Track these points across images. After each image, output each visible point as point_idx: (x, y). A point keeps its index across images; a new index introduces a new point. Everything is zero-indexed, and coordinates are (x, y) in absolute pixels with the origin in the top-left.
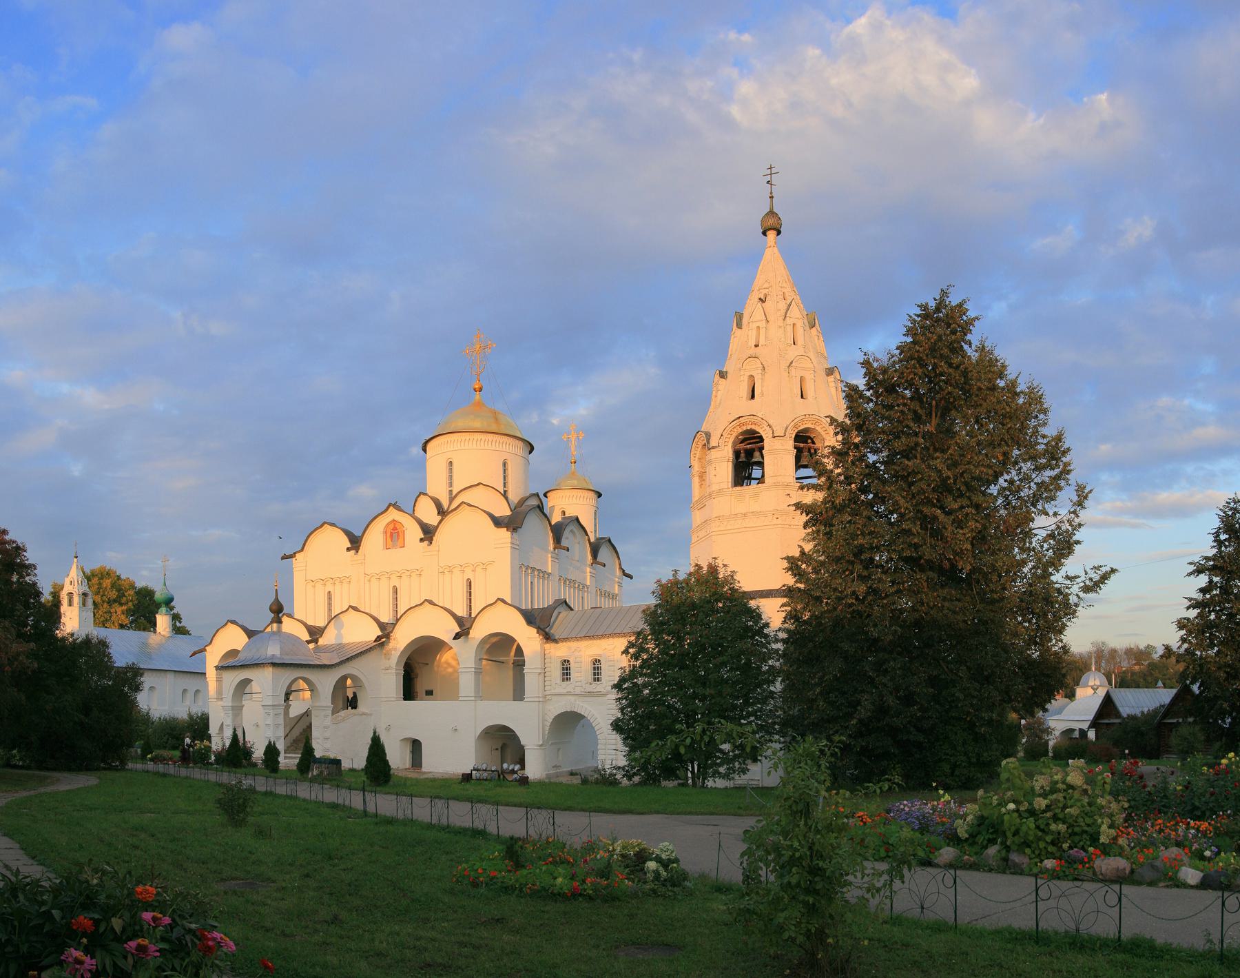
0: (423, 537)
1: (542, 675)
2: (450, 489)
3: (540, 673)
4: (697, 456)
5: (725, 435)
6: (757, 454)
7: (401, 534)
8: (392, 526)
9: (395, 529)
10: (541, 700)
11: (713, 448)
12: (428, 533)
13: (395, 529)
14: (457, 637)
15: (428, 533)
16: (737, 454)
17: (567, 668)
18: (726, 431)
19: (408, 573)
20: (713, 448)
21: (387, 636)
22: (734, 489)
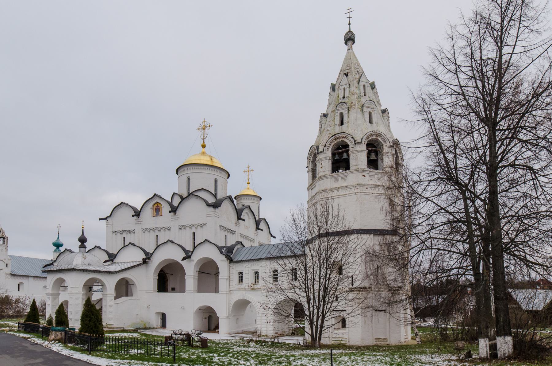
0: (171, 210)
1: (229, 280)
2: (188, 191)
3: (227, 279)
4: (311, 161)
5: (327, 145)
6: (345, 155)
7: (161, 209)
8: (156, 205)
9: (158, 206)
10: (228, 293)
11: (321, 152)
12: (174, 210)
13: (158, 206)
14: (184, 259)
15: (174, 210)
16: (333, 155)
17: (241, 276)
18: (328, 142)
19: (164, 229)
20: (321, 152)
21: (149, 258)
22: (333, 174)
